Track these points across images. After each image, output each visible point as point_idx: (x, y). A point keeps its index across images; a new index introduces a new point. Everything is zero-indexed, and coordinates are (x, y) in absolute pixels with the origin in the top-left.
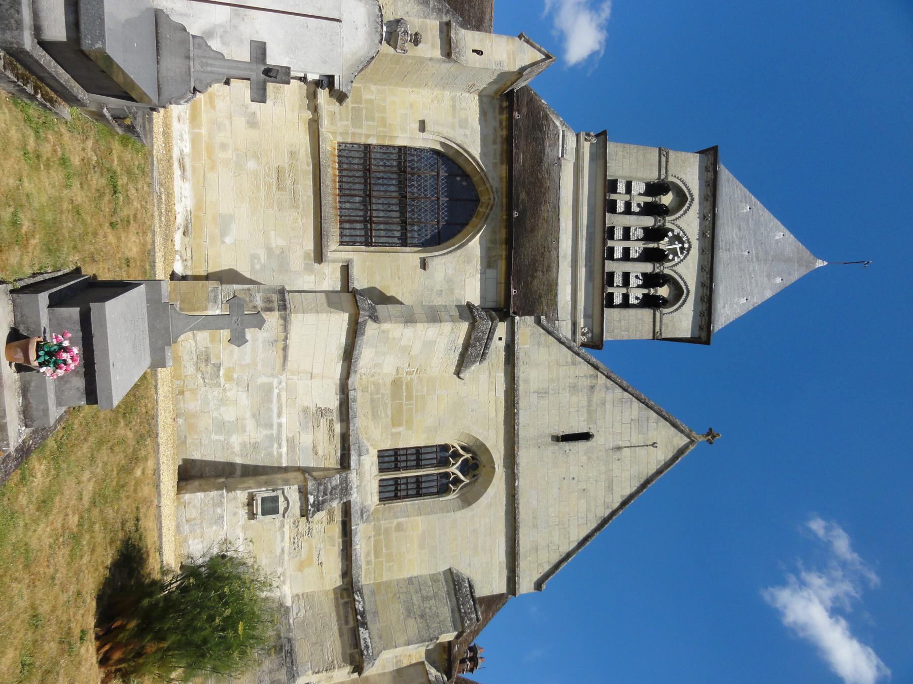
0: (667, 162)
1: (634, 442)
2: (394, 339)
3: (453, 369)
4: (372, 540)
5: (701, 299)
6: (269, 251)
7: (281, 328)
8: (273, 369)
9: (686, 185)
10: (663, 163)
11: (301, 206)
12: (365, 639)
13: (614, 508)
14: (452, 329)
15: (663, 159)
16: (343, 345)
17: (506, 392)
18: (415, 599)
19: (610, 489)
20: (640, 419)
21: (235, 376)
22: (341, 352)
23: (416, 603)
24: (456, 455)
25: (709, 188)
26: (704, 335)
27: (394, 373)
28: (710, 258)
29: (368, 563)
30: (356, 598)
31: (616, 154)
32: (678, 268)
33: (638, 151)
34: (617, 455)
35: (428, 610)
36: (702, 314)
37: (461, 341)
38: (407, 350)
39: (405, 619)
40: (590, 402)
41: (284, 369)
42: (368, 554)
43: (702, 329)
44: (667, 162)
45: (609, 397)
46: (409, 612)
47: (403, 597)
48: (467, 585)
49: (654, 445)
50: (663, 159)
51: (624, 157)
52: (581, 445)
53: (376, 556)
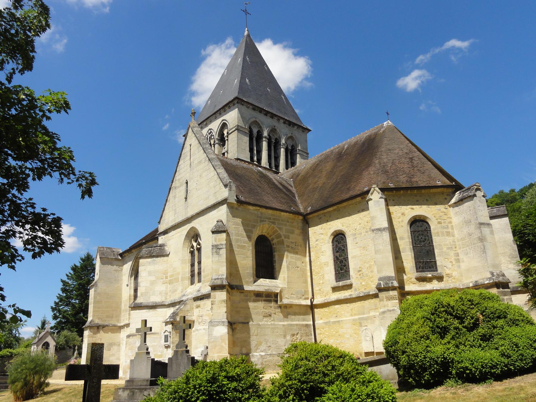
2: (146, 289)
3: (165, 258)
7: (134, 337)
8: (157, 338)
14: (143, 266)
16: (147, 310)
17: (174, 230)
21: (160, 353)
22: (151, 310)
26: (236, 102)
27: (166, 284)
28: (212, 117)
36: (230, 107)
37: (149, 260)
38: (153, 283)
41: (158, 333)
43: (234, 104)
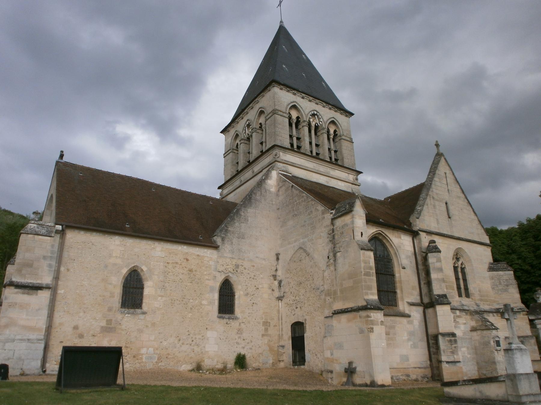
0: (281, 111)
1: (445, 182)
4: (484, 302)
5: (335, 111)
6: (409, 340)
9: (289, 104)
10: (281, 113)
11: (394, 324)
12: (518, 309)
13: (464, 197)
15: (279, 113)
18: (500, 288)
19: (459, 197)
20: (439, 178)
23: (502, 287)
24: (455, 263)
25: (290, 91)
29: (490, 305)
30: (502, 311)
31: (281, 140)
32: (325, 119)
33: (278, 127)
34: (450, 191)
35: (505, 283)
39: (509, 293)
40: (437, 200)
42: (488, 305)
44: (281, 111)
45: (434, 190)
46: (506, 291)
47: (500, 292)
48: (492, 266)
49: (445, 173)
50: (279, 113)
51: (281, 136)
52: (451, 207)
53: (487, 301)
